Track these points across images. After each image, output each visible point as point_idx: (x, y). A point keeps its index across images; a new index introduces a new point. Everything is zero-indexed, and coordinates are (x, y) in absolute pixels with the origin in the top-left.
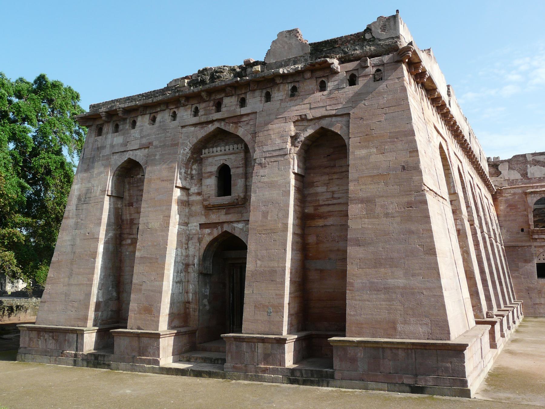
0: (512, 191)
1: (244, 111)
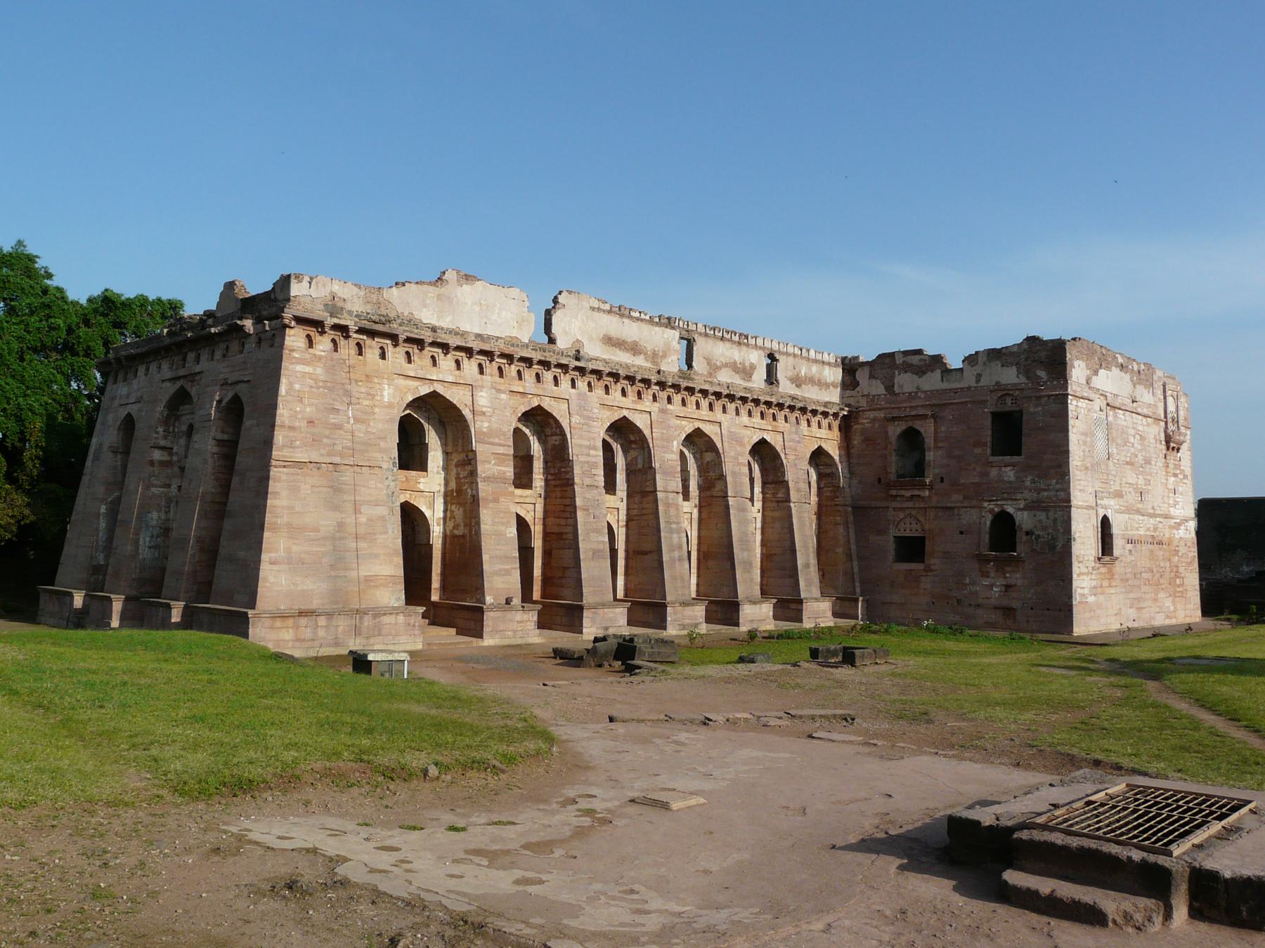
0: (872, 415)
1: (197, 369)
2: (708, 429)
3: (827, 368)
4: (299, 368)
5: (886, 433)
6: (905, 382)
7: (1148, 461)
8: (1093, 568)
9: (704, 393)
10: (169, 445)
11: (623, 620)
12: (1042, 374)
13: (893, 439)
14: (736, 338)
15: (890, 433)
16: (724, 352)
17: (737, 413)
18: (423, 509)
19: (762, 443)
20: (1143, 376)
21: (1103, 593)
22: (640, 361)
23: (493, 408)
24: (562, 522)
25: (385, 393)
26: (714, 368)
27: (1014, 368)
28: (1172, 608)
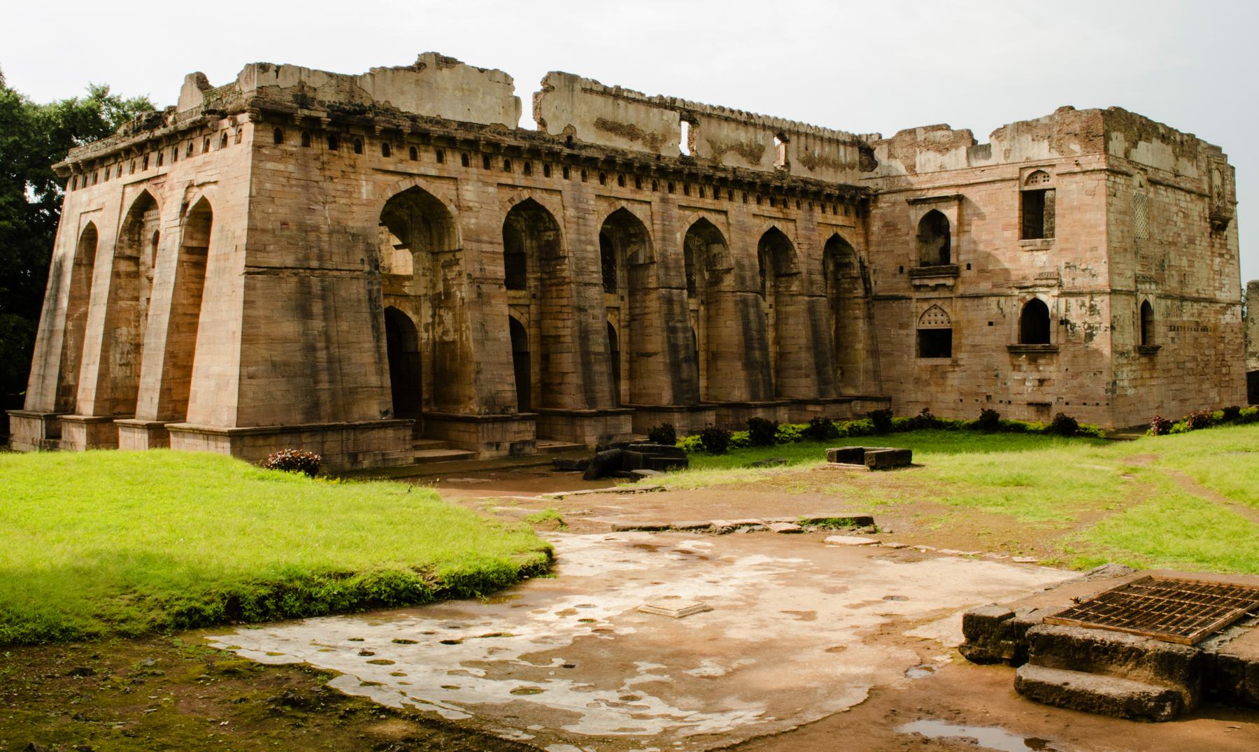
0: (893, 197)
1: (162, 170)
2: (712, 218)
3: (842, 148)
4: (270, 165)
5: (908, 217)
6: (927, 161)
7: (1191, 241)
8: (1134, 359)
9: (708, 179)
10: (134, 254)
11: (628, 428)
12: (1076, 147)
13: (916, 224)
14: (743, 118)
15: (913, 217)
16: (728, 134)
17: (745, 201)
18: (410, 314)
19: (774, 230)
20: (1186, 148)
21: (1143, 385)
22: (637, 148)
23: (478, 203)
24: (560, 324)
25: (363, 190)
26: (719, 151)
27: (1046, 143)
28: (1217, 399)
